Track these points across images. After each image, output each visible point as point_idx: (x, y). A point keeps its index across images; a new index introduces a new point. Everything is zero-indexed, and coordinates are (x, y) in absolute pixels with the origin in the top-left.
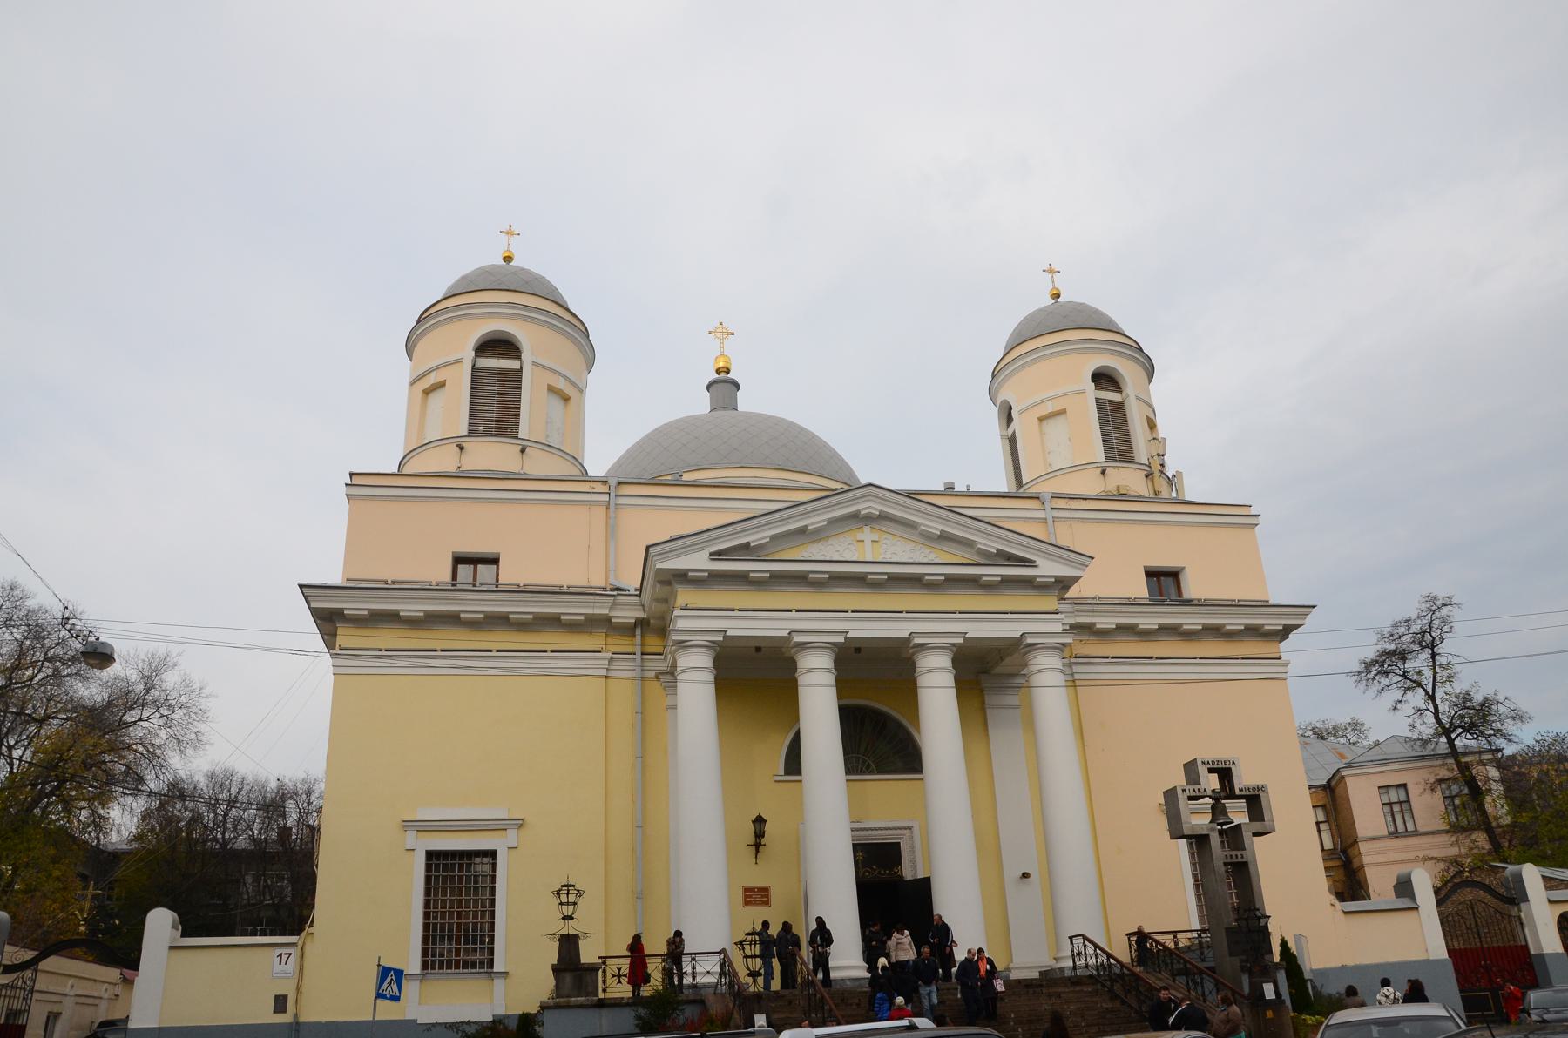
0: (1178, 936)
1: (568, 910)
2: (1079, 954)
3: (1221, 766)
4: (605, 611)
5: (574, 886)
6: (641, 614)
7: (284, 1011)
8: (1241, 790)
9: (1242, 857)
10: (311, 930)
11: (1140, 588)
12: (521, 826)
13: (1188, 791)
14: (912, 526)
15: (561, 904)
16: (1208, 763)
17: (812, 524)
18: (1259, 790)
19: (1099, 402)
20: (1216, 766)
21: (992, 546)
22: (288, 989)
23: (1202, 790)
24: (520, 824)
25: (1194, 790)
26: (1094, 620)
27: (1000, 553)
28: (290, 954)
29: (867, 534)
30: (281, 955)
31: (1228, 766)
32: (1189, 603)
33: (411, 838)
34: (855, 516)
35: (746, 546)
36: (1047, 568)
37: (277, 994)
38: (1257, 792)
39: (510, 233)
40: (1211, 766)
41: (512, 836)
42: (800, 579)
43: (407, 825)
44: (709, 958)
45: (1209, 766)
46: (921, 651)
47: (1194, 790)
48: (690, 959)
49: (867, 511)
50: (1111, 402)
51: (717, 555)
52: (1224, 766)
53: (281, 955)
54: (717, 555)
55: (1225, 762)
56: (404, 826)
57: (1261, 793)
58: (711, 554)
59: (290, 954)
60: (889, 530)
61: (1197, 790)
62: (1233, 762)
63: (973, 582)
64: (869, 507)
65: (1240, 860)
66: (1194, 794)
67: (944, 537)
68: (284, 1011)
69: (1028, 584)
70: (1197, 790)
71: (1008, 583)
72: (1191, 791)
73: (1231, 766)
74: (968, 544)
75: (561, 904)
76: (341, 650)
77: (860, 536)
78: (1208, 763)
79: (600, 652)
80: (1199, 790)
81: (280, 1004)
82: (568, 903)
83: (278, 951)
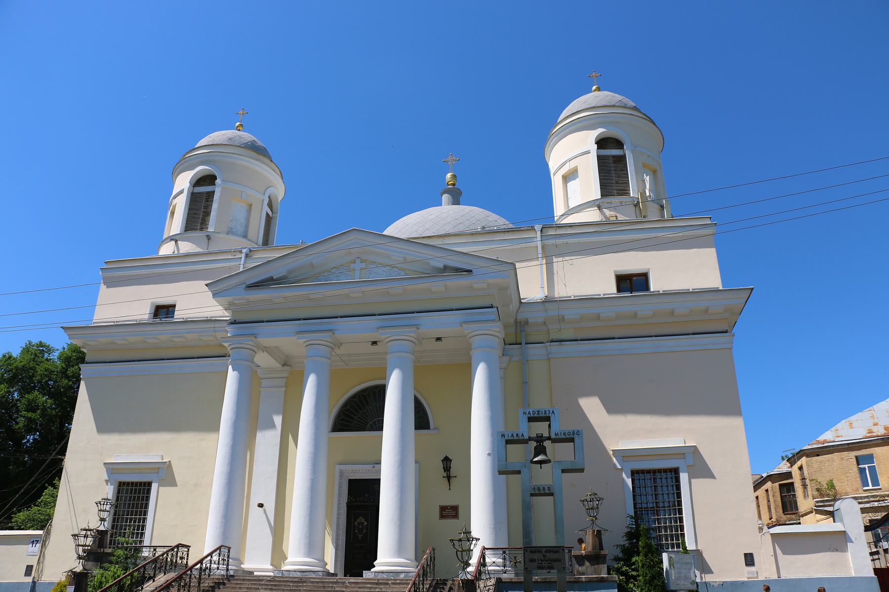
3: (541, 415)
11: (611, 288)
13: (506, 436)
15: (101, 510)
16: (529, 413)
18: (574, 434)
19: (600, 158)
20: (536, 415)
22: (33, 562)
25: (512, 435)
30: (33, 542)
31: (547, 415)
38: (571, 436)
40: (532, 415)
45: (529, 416)
47: (512, 435)
50: (614, 157)
52: (544, 415)
55: (545, 411)
57: (576, 436)
61: (515, 435)
62: (553, 412)
66: (512, 438)
70: (515, 435)
72: (510, 436)
73: (550, 415)
78: (529, 413)
79: (225, 357)
80: (517, 435)
81: (29, 570)
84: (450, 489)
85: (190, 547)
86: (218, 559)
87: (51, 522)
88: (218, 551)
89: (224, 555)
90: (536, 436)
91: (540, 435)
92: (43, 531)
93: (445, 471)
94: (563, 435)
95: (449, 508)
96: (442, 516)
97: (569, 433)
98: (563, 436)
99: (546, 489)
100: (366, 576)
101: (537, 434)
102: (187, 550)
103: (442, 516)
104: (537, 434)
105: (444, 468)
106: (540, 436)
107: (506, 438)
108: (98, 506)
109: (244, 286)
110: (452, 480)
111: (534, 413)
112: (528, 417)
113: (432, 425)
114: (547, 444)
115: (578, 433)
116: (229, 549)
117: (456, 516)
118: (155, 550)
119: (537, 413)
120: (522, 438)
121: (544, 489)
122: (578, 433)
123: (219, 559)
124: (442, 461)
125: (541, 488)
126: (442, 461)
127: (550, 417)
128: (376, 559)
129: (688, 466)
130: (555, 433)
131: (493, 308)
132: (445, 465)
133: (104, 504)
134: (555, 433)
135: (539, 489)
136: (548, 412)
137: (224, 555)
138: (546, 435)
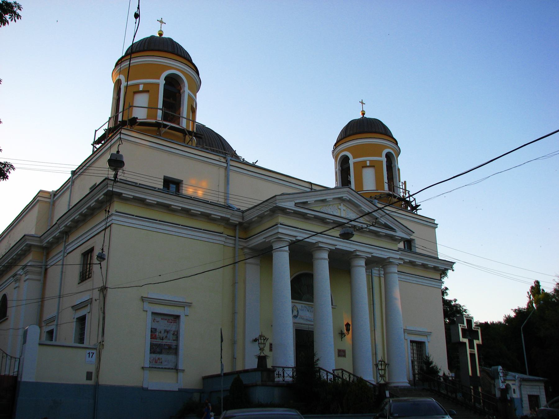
1: (262, 346)
4: (229, 216)
5: (264, 336)
6: (241, 220)
7: (91, 379)
8: (474, 328)
9: (474, 351)
22: (92, 369)
24: (189, 305)
30: (89, 353)
33: (147, 306)
36: (399, 234)
37: (88, 371)
39: (161, 22)
41: (187, 310)
46: (357, 257)
48: (282, 369)
49: (345, 198)
53: (89, 353)
58: (296, 204)
60: (348, 206)
64: (347, 196)
65: (473, 352)
68: (91, 379)
71: (387, 236)
76: (116, 212)
81: (89, 376)
83: (88, 351)
118: (283, 369)
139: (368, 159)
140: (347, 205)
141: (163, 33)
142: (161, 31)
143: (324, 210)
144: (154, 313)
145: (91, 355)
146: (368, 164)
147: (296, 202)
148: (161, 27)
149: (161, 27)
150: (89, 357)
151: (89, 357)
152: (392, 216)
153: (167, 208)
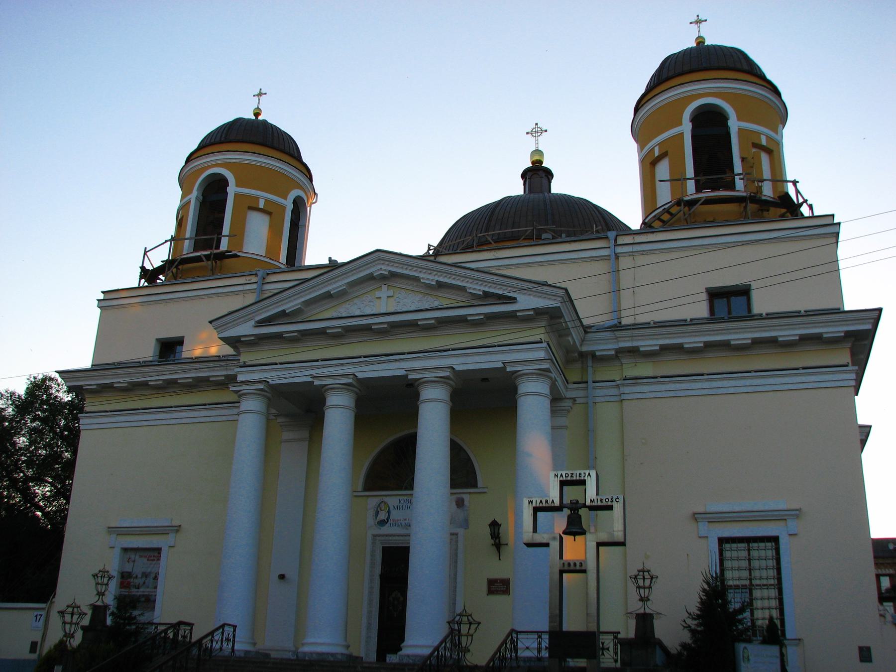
0: (543, 637)
2: (228, 640)
10: (54, 600)
11: (702, 310)
12: (177, 531)
14: (416, 279)
16: (562, 475)
17: (334, 289)
18: (612, 501)
20: (569, 478)
21: (478, 288)
22: (39, 639)
23: (550, 502)
24: (177, 529)
25: (541, 502)
26: (635, 344)
27: (487, 295)
28: (41, 615)
29: (384, 292)
30: (36, 616)
31: (582, 478)
32: (760, 317)
34: (371, 278)
35: (283, 314)
36: (526, 302)
38: (609, 503)
40: (564, 478)
41: (170, 539)
42: (321, 333)
43: (111, 530)
44: (528, 636)
45: (561, 479)
47: (541, 502)
51: (261, 323)
52: (578, 478)
53: (36, 616)
54: (261, 323)
56: (109, 532)
59: (41, 615)
60: (401, 286)
63: (462, 321)
64: (381, 269)
67: (440, 285)
69: (511, 317)
72: (538, 503)
73: (586, 478)
74: (463, 289)
75: (97, 584)
77: (378, 294)
78: (562, 475)
80: (547, 501)
82: (102, 584)
83: (36, 613)
84: (500, 559)
85: (193, 624)
86: (220, 638)
87: (55, 595)
88: (221, 630)
89: (229, 635)
90: (569, 502)
91: (575, 501)
92: (45, 604)
93: (492, 538)
94: (599, 501)
95: (498, 581)
96: (490, 592)
97: (607, 500)
98: (599, 503)
99: (578, 564)
100: (389, 661)
101: (571, 500)
102: (190, 628)
103: (490, 592)
104: (571, 500)
105: (491, 534)
106: (574, 503)
107: (534, 504)
108: (95, 578)
109: (252, 323)
110: (503, 548)
111: (567, 475)
112: (560, 481)
113: (480, 483)
114: (583, 512)
115: (617, 500)
116: (235, 627)
117: (506, 591)
119: (570, 476)
120: (553, 505)
121: (575, 564)
122: (617, 500)
123: (222, 639)
124: (490, 525)
125: (572, 564)
126: (490, 525)
127: (585, 480)
128: (403, 640)
129: (790, 535)
130: (591, 500)
131: (541, 342)
132: (493, 532)
133: (101, 577)
134: (591, 500)
135: (569, 564)
136: (583, 475)
137: (229, 635)
138: (581, 501)
139: (263, 197)
140: (394, 284)
141: (704, 39)
142: (258, 108)
143: (343, 311)
144: (125, 550)
145: (39, 617)
146: (261, 206)
147: (257, 319)
148: (259, 103)
149: (259, 103)
150: (36, 621)
151: (36, 621)
152: (486, 270)
153: (169, 386)
